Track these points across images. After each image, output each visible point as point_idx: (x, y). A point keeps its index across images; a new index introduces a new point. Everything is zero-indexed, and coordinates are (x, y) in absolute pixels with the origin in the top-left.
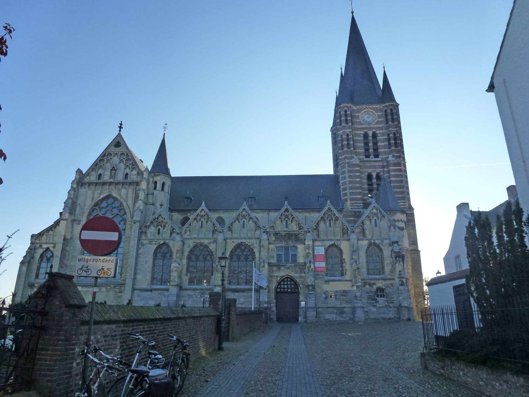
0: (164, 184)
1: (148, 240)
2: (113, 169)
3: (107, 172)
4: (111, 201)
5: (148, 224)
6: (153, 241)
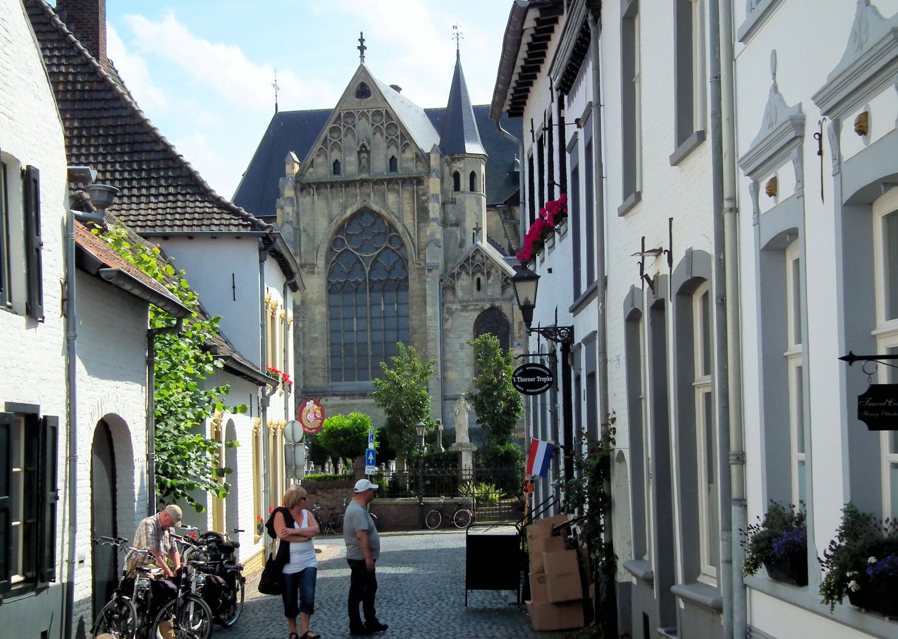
0: (473, 175)
1: (460, 302)
2: (364, 150)
3: (351, 155)
4: (368, 220)
5: (455, 271)
6: (470, 305)
